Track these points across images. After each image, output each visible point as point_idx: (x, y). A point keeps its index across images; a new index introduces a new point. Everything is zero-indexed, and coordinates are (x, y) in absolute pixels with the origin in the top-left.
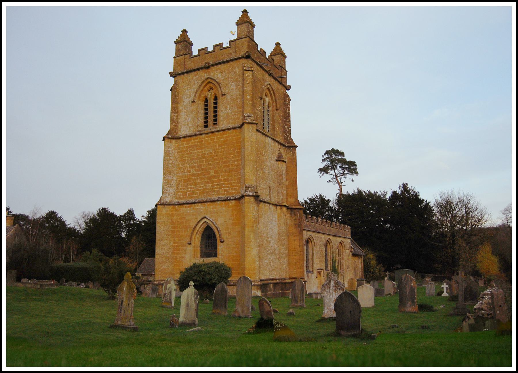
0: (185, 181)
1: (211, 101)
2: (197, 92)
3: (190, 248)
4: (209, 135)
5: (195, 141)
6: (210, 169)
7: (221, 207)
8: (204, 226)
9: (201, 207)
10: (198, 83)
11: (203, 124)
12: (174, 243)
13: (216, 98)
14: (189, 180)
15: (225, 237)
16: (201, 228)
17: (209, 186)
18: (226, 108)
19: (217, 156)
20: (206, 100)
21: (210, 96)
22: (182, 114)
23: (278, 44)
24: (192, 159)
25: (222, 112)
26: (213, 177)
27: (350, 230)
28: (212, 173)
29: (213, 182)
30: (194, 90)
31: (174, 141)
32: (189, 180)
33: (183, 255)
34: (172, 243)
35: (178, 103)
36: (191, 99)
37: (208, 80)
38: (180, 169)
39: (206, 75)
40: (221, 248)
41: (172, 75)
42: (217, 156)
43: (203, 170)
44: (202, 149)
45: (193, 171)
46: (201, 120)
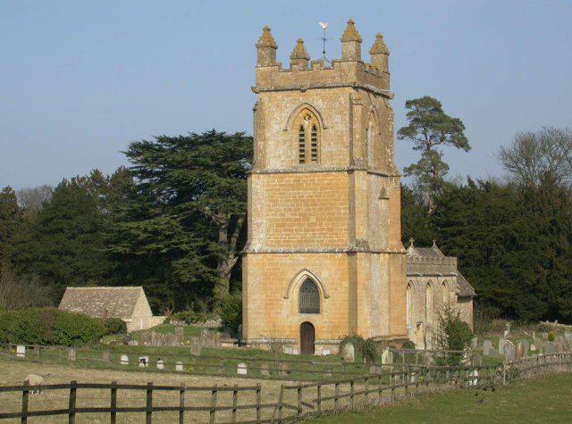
0: (278, 225)
1: (309, 132)
2: (290, 118)
3: (286, 303)
4: (307, 174)
5: (290, 179)
6: (310, 214)
7: (327, 260)
8: (306, 277)
9: (300, 257)
10: (289, 110)
11: (298, 158)
12: (267, 296)
13: (314, 128)
14: (283, 225)
15: (329, 292)
16: (300, 279)
17: (309, 235)
18: (329, 144)
19: (319, 200)
20: (302, 129)
21: (307, 124)
22: (271, 143)
23: (379, 37)
24: (288, 201)
25: (325, 148)
26: (315, 224)
27: (456, 263)
28: (313, 220)
29: (314, 230)
30: (285, 115)
31: (262, 176)
32: (283, 225)
33: (279, 310)
34: (264, 297)
35: (264, 128)
36: (283, 126)
37: (306, 106)
38: (271, 210)
39: (301, 99)
40: (325, 304)
41: (254, 90)
42: (319, 200)
43: (300, 215)
44: (299, 189)
45: (288, 215)
46: (295, 153)
